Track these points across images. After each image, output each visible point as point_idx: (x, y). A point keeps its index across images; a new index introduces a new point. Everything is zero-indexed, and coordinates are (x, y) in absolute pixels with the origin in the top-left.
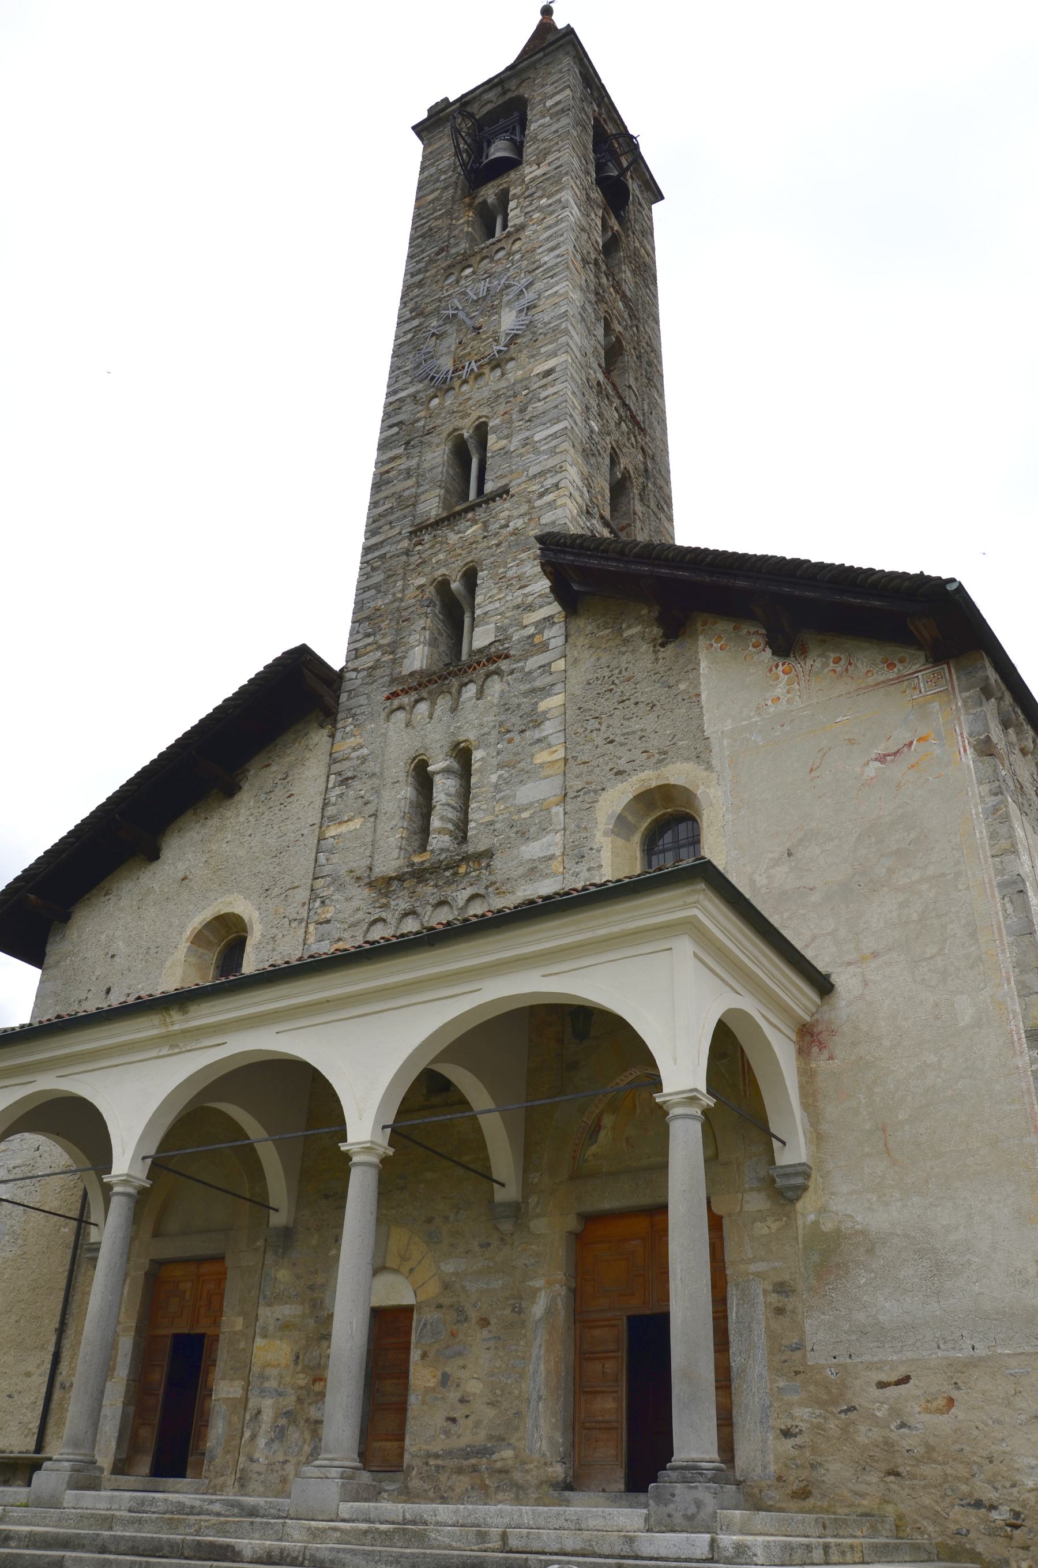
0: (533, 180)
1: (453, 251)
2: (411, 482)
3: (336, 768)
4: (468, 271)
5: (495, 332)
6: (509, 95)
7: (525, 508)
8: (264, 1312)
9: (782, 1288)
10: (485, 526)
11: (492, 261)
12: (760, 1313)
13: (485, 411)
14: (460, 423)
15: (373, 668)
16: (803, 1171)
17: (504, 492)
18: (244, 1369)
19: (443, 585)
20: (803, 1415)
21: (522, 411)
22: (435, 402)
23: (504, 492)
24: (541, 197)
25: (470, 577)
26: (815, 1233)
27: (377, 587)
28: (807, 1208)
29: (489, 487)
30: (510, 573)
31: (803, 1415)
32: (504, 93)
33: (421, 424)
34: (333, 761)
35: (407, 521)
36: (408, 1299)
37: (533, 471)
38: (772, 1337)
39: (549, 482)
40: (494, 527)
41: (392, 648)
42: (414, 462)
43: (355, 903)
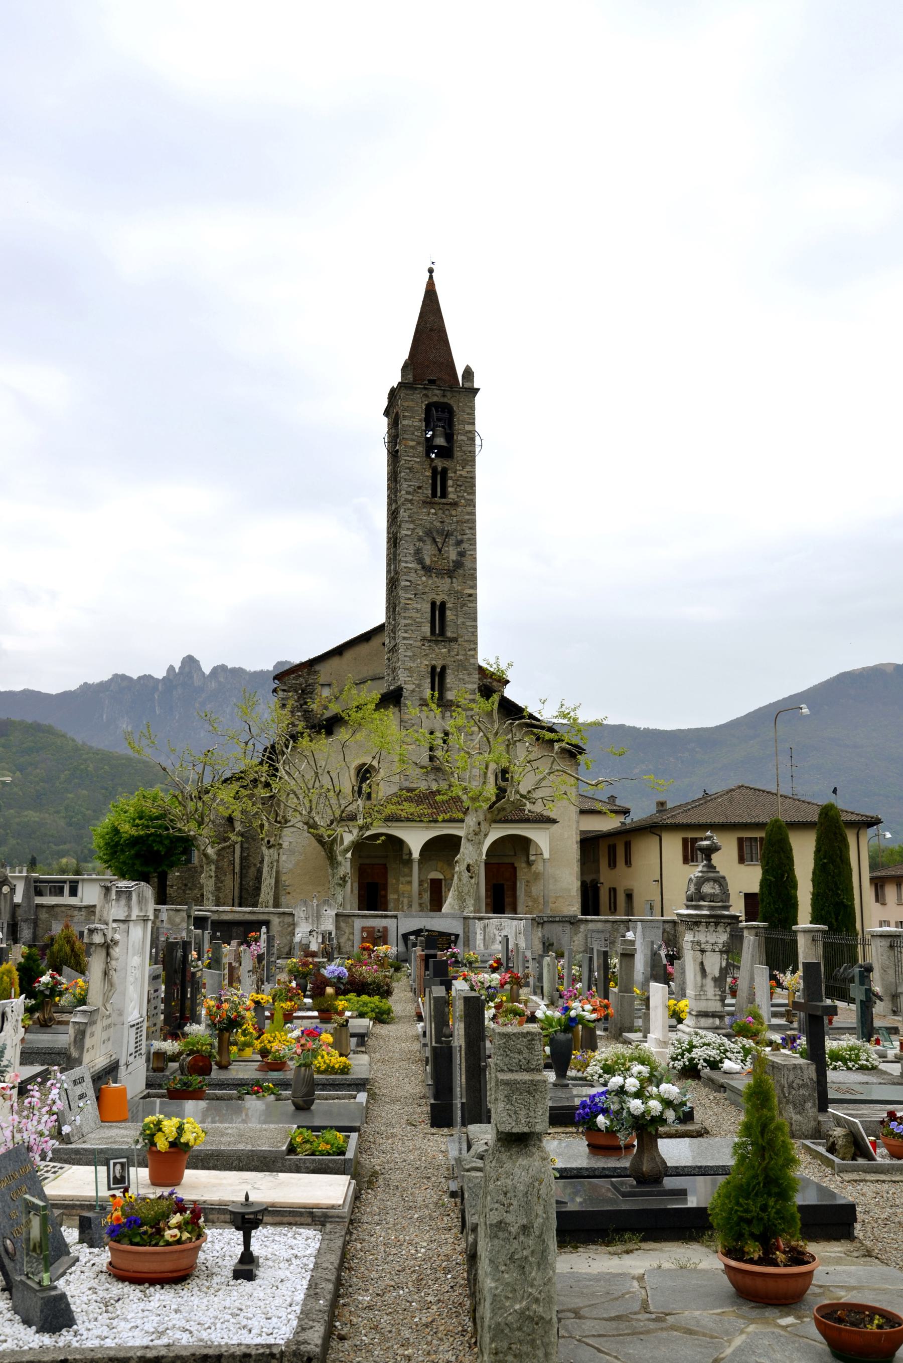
0: (461, 476)
1: (425, 492)
2: (419, 615)
3: (403, 724)
4: (433, 511)
5: (448, 557)
6: (446, 400)
7: (463, 652)
8: (402, 879)
9: (528, 882)
10: (449, 651)
11: (444, 513)
12: (523, 886)
13: (446, 598)
14: (435, 596)
15: (413, 691)
16: (534, 861)
17: (455, 640)
18: (397, 891)
19: (433, 668)
20: (530, 904)
21: (462, 607)
22: (424, 578)
23: (455, 640)
24: (465, 491)
25: (444, 668)
26: (535, 872)
27: (409, 657)
28: (534, 868)
29: (449, 634)
30: (461, 676)
31: (530, 904)
32: (444, 396)
33: (420, 587)
34: (401, 721)
35: (419, 633)
36: (441, 877)
37: (466, 638)
38: (526, 890)
39: (472, 646)
40: (452, 654)
41: (419, 686)
42: (419, 606)
43: (416, 773)
